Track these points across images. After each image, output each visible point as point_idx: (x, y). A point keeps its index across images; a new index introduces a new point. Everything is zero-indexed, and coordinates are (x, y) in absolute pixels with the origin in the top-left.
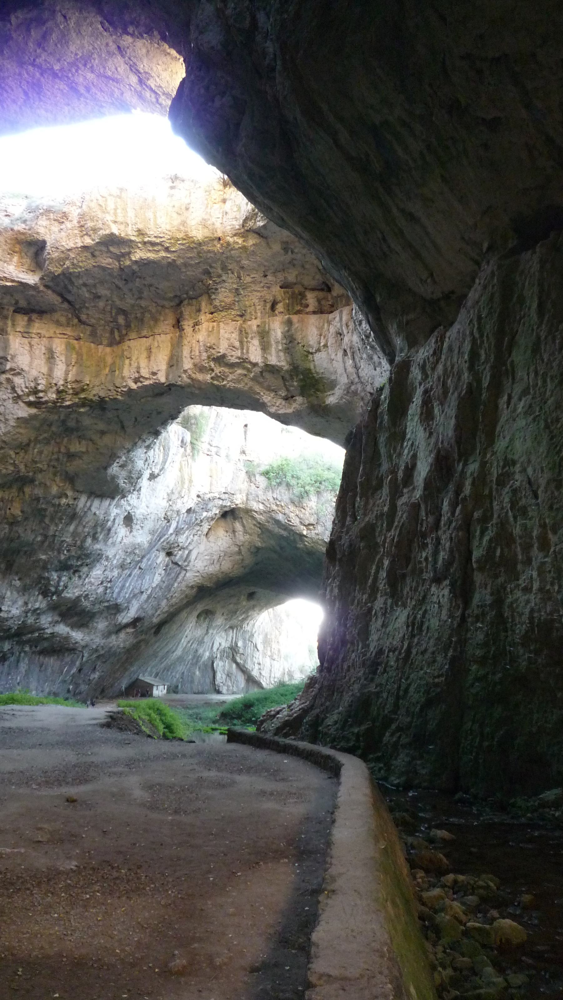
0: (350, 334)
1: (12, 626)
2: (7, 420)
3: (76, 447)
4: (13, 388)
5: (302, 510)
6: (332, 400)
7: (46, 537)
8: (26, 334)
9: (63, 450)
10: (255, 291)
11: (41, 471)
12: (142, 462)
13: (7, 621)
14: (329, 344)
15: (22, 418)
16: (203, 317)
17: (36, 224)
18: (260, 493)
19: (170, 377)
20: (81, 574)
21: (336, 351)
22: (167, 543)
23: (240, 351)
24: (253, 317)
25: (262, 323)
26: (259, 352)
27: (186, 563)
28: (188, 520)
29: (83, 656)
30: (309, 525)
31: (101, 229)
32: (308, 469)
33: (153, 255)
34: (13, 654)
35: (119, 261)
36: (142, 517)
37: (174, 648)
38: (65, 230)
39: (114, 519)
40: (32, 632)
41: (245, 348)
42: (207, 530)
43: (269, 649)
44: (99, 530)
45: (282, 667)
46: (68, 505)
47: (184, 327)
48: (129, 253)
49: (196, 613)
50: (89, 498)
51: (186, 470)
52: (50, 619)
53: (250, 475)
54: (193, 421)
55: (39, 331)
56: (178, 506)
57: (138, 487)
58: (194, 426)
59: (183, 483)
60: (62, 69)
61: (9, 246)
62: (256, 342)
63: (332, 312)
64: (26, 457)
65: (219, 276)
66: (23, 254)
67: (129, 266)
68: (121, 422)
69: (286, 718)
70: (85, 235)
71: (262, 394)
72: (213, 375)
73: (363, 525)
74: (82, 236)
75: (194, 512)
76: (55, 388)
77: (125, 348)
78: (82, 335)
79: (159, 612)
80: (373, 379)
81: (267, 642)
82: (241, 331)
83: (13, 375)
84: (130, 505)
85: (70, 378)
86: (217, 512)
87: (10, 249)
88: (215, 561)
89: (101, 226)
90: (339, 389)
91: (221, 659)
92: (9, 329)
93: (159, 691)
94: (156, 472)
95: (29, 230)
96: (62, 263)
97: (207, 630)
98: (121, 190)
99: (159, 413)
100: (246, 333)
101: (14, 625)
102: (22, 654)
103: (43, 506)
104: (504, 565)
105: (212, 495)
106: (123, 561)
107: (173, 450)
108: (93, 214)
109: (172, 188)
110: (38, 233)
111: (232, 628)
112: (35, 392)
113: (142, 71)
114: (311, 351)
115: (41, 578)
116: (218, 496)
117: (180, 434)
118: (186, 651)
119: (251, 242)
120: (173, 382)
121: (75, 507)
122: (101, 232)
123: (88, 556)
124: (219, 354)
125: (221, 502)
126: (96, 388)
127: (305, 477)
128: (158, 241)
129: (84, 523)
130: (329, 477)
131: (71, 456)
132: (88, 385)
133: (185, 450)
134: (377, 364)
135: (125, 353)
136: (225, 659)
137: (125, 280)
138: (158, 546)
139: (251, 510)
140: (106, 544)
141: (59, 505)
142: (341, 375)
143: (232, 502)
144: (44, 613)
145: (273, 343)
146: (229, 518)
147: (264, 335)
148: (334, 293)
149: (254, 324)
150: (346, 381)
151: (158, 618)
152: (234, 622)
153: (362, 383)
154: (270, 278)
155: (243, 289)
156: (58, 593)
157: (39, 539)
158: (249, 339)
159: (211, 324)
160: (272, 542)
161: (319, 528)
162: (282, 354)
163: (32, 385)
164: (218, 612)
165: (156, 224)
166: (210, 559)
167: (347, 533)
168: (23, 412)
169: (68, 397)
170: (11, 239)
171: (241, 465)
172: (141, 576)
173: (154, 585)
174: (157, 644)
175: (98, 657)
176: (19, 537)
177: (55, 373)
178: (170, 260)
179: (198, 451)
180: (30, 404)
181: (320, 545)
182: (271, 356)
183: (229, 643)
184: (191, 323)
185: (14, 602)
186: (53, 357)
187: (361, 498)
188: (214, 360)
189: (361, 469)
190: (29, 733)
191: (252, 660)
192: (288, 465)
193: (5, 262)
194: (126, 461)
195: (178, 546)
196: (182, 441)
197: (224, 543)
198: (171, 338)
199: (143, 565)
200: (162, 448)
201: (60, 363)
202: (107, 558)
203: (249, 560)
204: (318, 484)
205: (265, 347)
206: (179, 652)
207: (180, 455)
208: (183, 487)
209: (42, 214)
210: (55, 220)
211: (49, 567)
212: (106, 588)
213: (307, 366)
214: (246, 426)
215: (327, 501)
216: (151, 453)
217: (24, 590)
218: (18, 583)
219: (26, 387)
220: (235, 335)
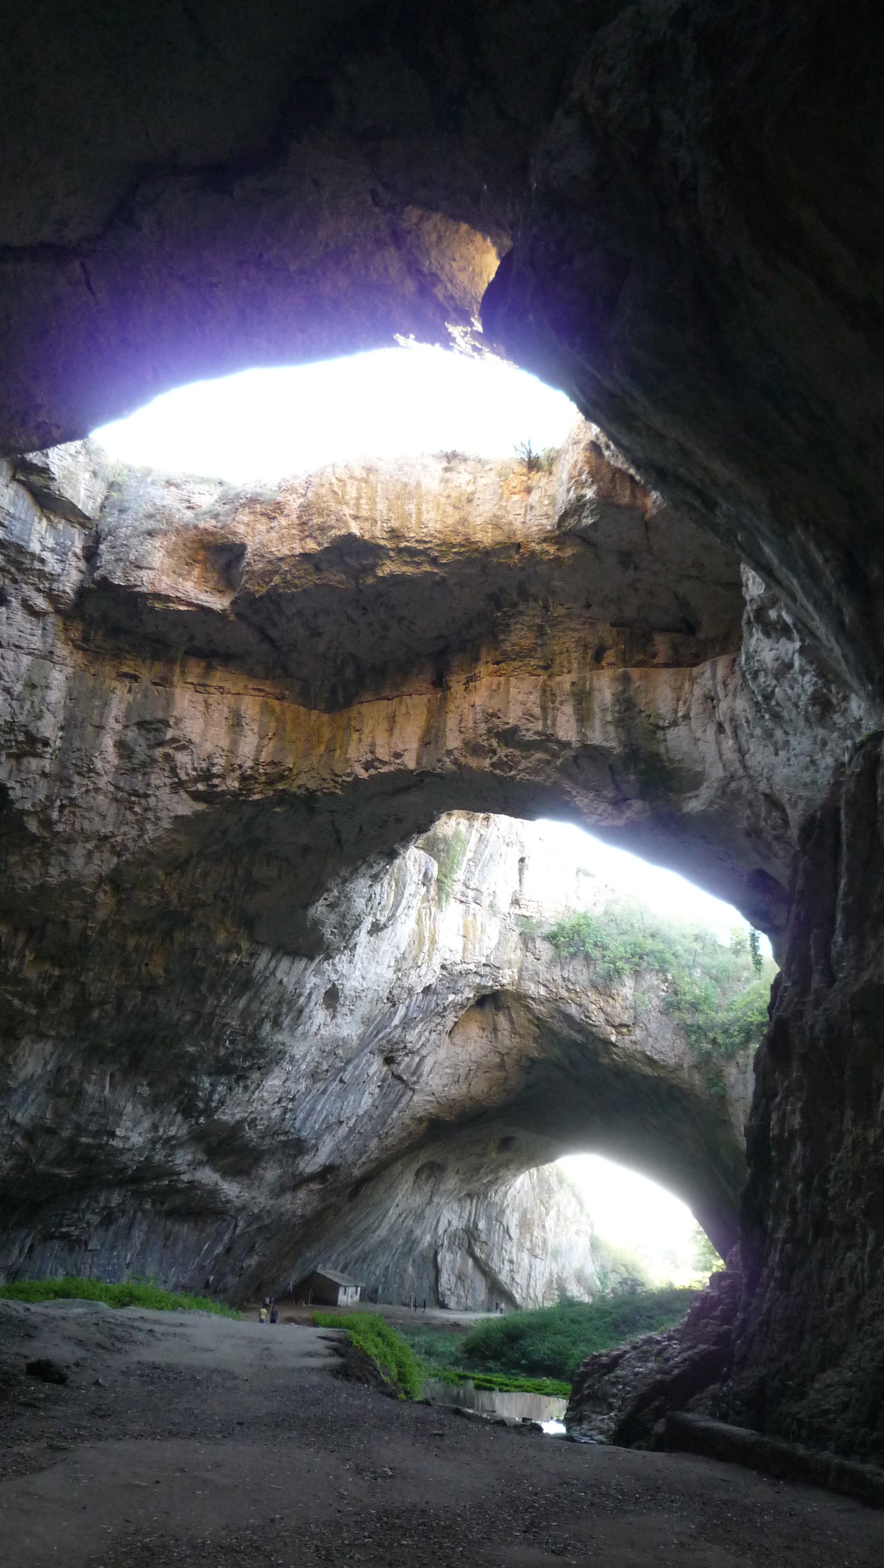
0: (730, 698)
1: (129, 1163)
2: (158, 819)
4: (173, 770)
5: (610, 1000)
6: (693, 806)
7: (198, 1015)
8: (201, 687)
9: (240, 872)
10: (571, 629)
11: (203, 905)
12: (363, 901)
13: (121, 1154)
14: (692, 715)
15: (182, 817)
16: (482, 669)
17: (234, 519)
18: (542, 968)
19: (424, 761)
20: (249, 1083)
21: (705, 725)
22: (388, 1041)
23: (541, 722)
24: (565, 670)
25: (580, 678)
26: (573, 724)
27: (415, 1079)
28: (424, 1005)
29: (236, 1226)
30: (622, 1025)
31: (332, 527)
32: (620, 934)
33: (411, 569)
34: (124, 1212)
35: (356, 578)
36: (353, 993)
37: (377, 1223)
38: (277, 529)
39: (310, 994)
40: (159, 1177)
41: (550, 717)
42: (452, 1024)
43: (528, 1236)
44: (284, 1010)
45: (548, 1270)
46: (240, 963)
47: (450, 684)
48: (375, 566)
49: (415, 1167)
50: (273, 955)
51: (427, 923)
52: (189, 1157)
53: (526, 939)
54: (441, 846)
55: (220, 684)
56: (410, 981)
57: (352, 942)
58: (442, 854)
59: (421, 943)
60: (301, 272)
61: (189, 552)
62: (568, 709)
63: (695, 665)
64: (182, 881)
65: (514, 605)
66: (208, 565)
67: (372, 585)
68: (337, 832)
69: (658, 1377)
70: (307, 536)
71: (574, 793)
72: (495, 759)
73: (856, 988)
74: (302, 539)
75: (436, 993)
76: (239, 772)
77: (354, 714)
78: (287, 693)
79: (364, 1159)
80: (772, 768)
81: (525, 1225)
82: (544, 692)
83: (175, 748)
84: (336, 972)
85: (264, 757)
86: (471, 996)
87: (189, 556)
88: (462, 1078)
89: (333, 522)
90: (708, 787)
91: (450, 1249)
92: (176, 679)
93: (348, 1297)
94: (383, 920)
95: (222, 528)
96: (267, 580)
97: (431, 1197)
98: (369, 470)
99: (399, 821)
100: (554, 695)
102: (139, 1215)
103: (201, 964)
105: (465, 966)
106: (317, 1067)
107: (410, 889)
108: (323, 505)
109: (447, 470)
110: (235, 533)
111: (470, 1196)
112: (206, 776)
113: (426, 271)
114: (661, 723)
115: (184, 1084)
116: (475, 970)
117: (423, 863)
118: (394, 1231)
119: (569, 552)
120: (429, 768)
121: (251, 968)
122: (334, 533)
123: (262, 1053)
124: (507, 727)
125: (478, 980)
126: (303, 776)
127: (617, 947)
128: (421, 547)
129: (263, 997)
130: (656, 948)
132: (290, 770)
133: (428, 891)
134: (780, 744)
135: (353, 723)
136: (455, 1248)
137: (364, 608)
138: (373, 1045)
139: (526, 996)
140: (293, 1035)
141: (227, 961)
142: (712, 765)
143: (495, 980)
144: (181, 1145)
145: (597, 710)
146: (489, 1008)
147: (582, 698)
148: (701, 636)
149: (565, 681)
150: (721, 774)
151: (362, 1169)
152: (474, 1186)
153: (750, 777)
154: (595, 609)
155: (551, 626)
156: (209, 1112)
157: (188, 1018)
158: (557, 704)
159: (496, 680)
160: (557, 1052)
161: (638, 1032)
162: (611, 728)
163: (204, 765)
164: (450, 1168)
165: (419, 522)
166: (453, 1074)
167: (817, 1004)
168: (185, 807)
169: (258, 787)
170: (193, 542)
171: (511, 922)
172: (342, 1096)
173: (361, 1112)
174: (353, 1215)
175: (259, 1230)
176: (156, 1012)
177: (241, 749)
178: (437, 578)
179: (447, 896)
180: (196, 796)
181: (639, 1061)
182: (594, 731)
183: (465, 1222)
184: (463, 678)
185: (136, 1123)
186: (239, 725)
187: (846, 937)
188: (497, 735)
189: (843, 882)
190: (199, 1383)
191: (500, 1254)
192: (588, 925)
193: (180, 575)
194: (339, 898)
195: (405, 1047)
196: (425, 875)
197: (479, 1049)
198: (429, 700)
199: (347, 1076)
200: (393, 883)
201: (250, 733)
202: (292, 1059)
204: (636, 960)
205: (583, 717)
207: (419, 897)
208: (421, 951)
209: (243, 506)
210: (262, 514)
211: (199, 1066)
212: (285, 1111)
214: (522, 860)
215: (651, 988)
216: (377, 888)
217: (154, 1103)
218: (145, 1091)
219: (195, 769)
220: (535, 697)
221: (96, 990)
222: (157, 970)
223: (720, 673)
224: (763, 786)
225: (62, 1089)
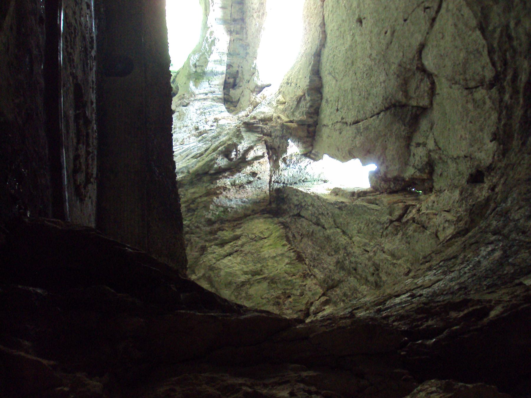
62: (219, 58)
147: (220, 62)
188: (214, 40)
213: (205, 78)
223: (219, 96)
224: (191, 103)
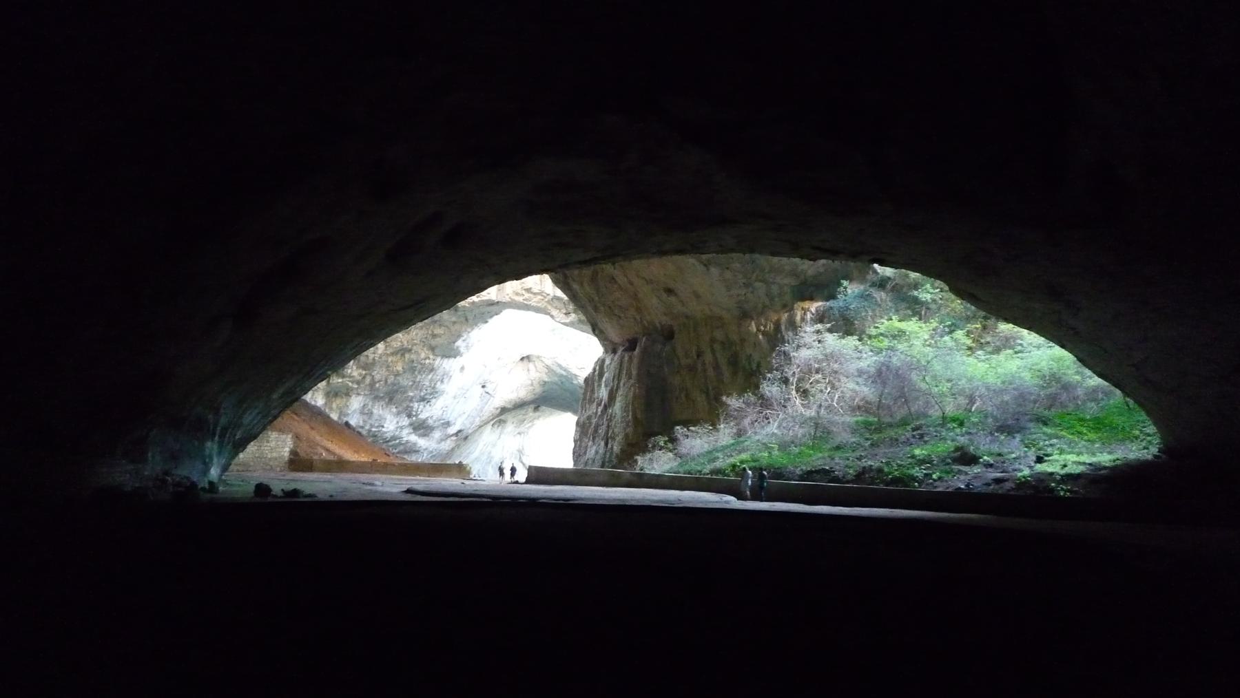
3: (438, 331)
101: (388, 435)
104: (613, 439)
131: (434, 336)
152: (522, 429)
156: (416, 416)
203: (538, 390)
206: (476, 454)
217: (398, 413)
218: (394, 410)
221: (377, 377)
222: (400, 368)
225: (366, 412)
